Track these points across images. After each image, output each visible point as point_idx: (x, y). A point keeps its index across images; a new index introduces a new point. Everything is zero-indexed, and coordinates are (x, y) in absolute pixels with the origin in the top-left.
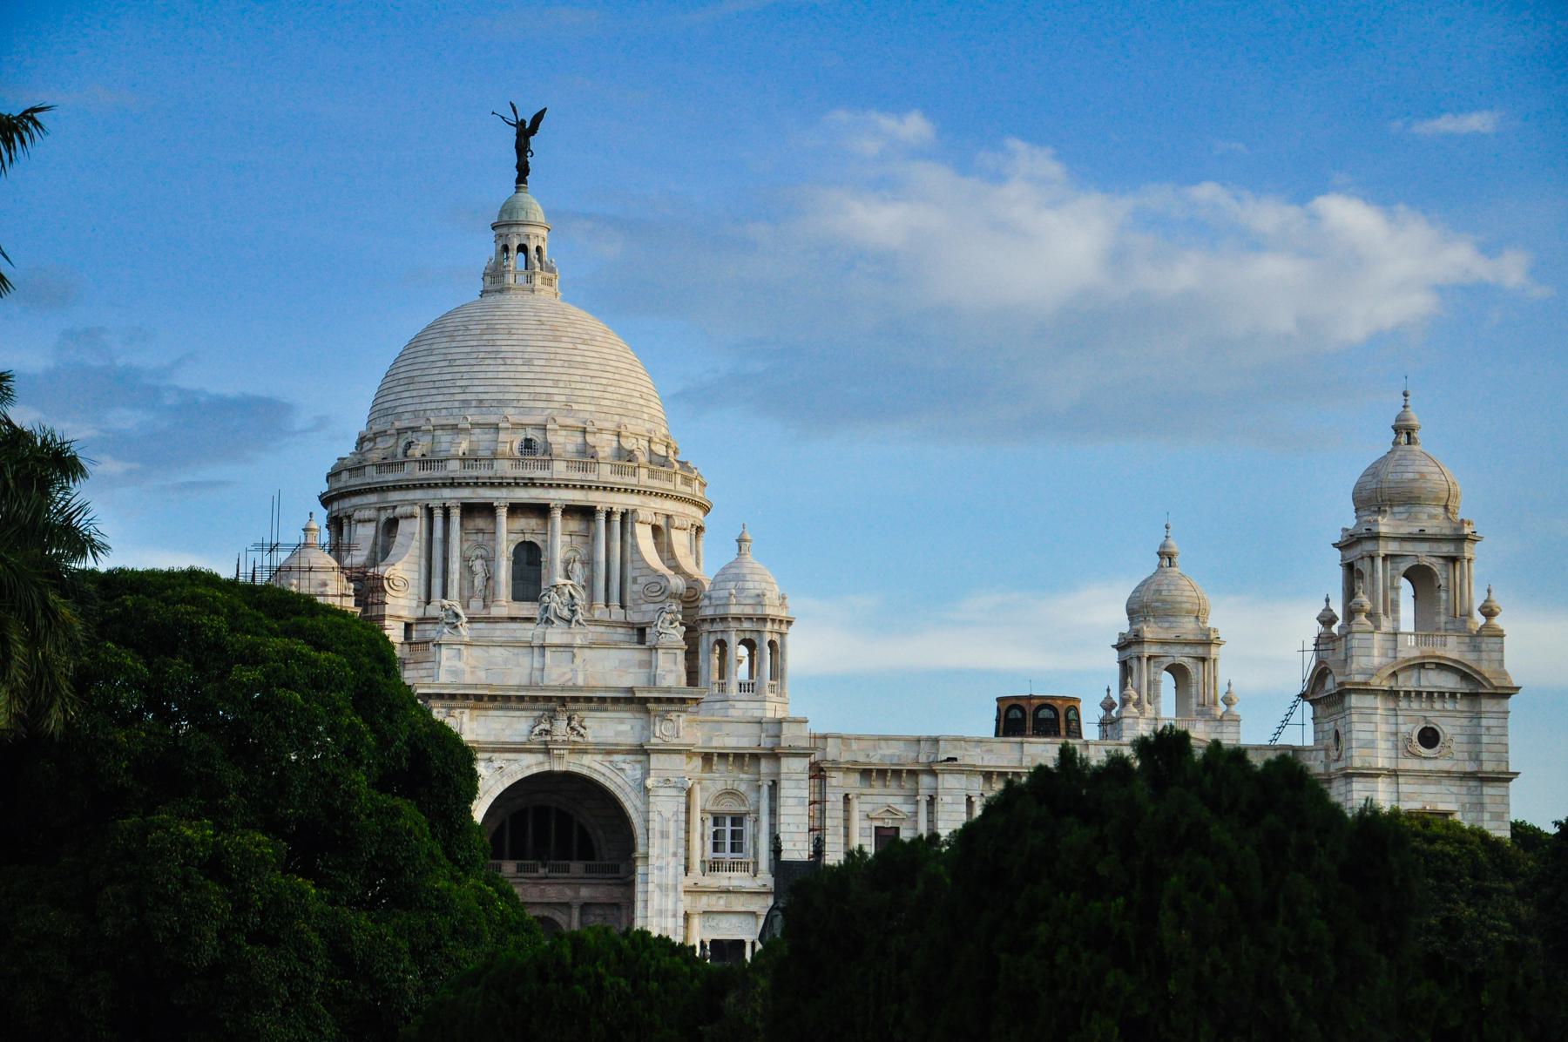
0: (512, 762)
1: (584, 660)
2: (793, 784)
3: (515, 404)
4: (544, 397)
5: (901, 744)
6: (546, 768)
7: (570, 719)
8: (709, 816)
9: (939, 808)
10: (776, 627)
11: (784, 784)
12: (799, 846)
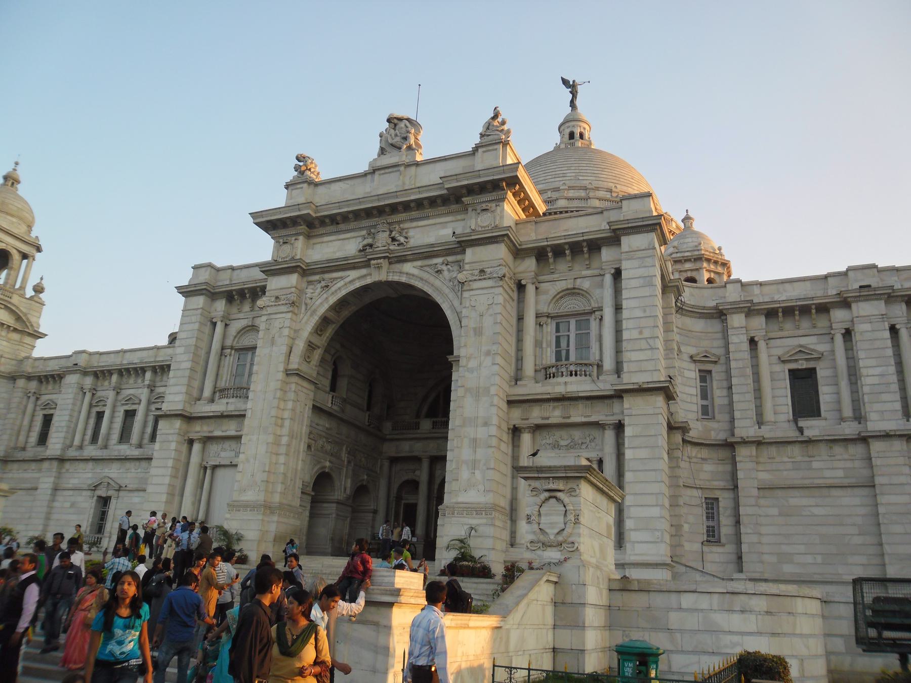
0: (339, 280)
1: (410, 177)
2: (636, 263)
3: (543, 182)
4: (561, 175)
5: (808, 284)
6: (369, 281)
7: (391, 232)
8: (549, 320)
9: (856, 337)
10: (712, 267)
11: (625, 265)
12: (647, 333)
